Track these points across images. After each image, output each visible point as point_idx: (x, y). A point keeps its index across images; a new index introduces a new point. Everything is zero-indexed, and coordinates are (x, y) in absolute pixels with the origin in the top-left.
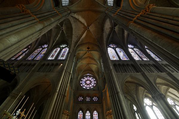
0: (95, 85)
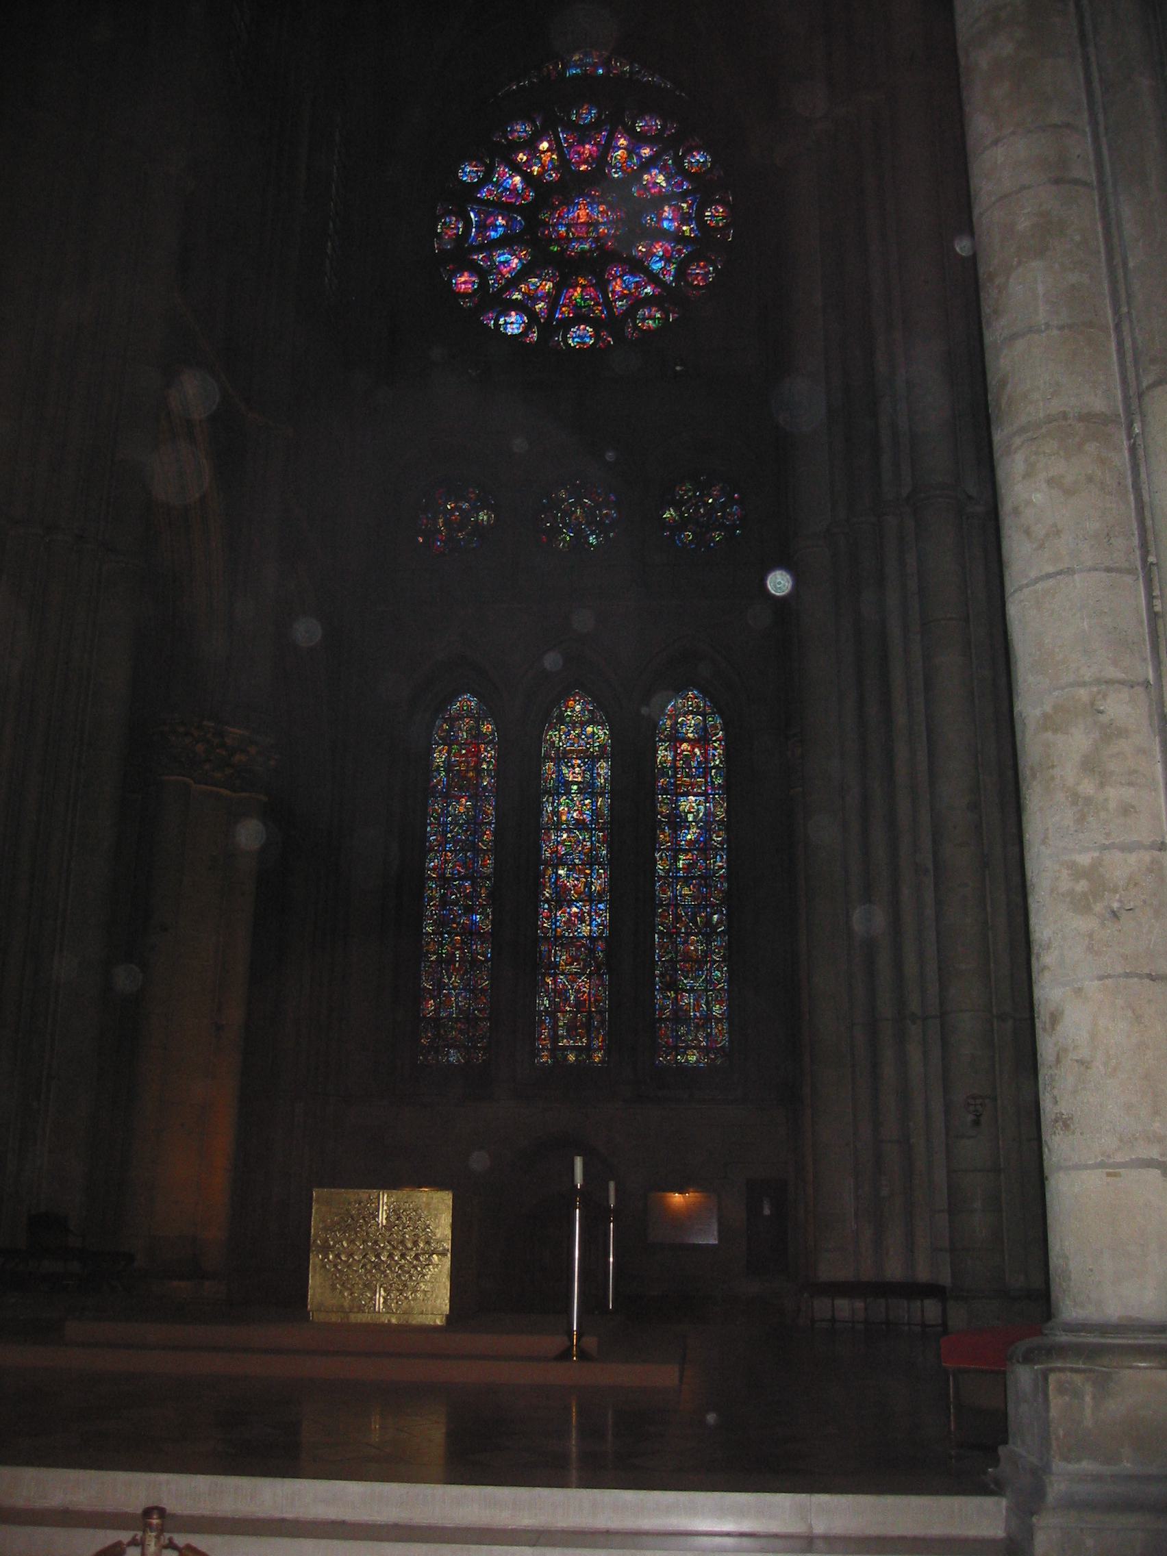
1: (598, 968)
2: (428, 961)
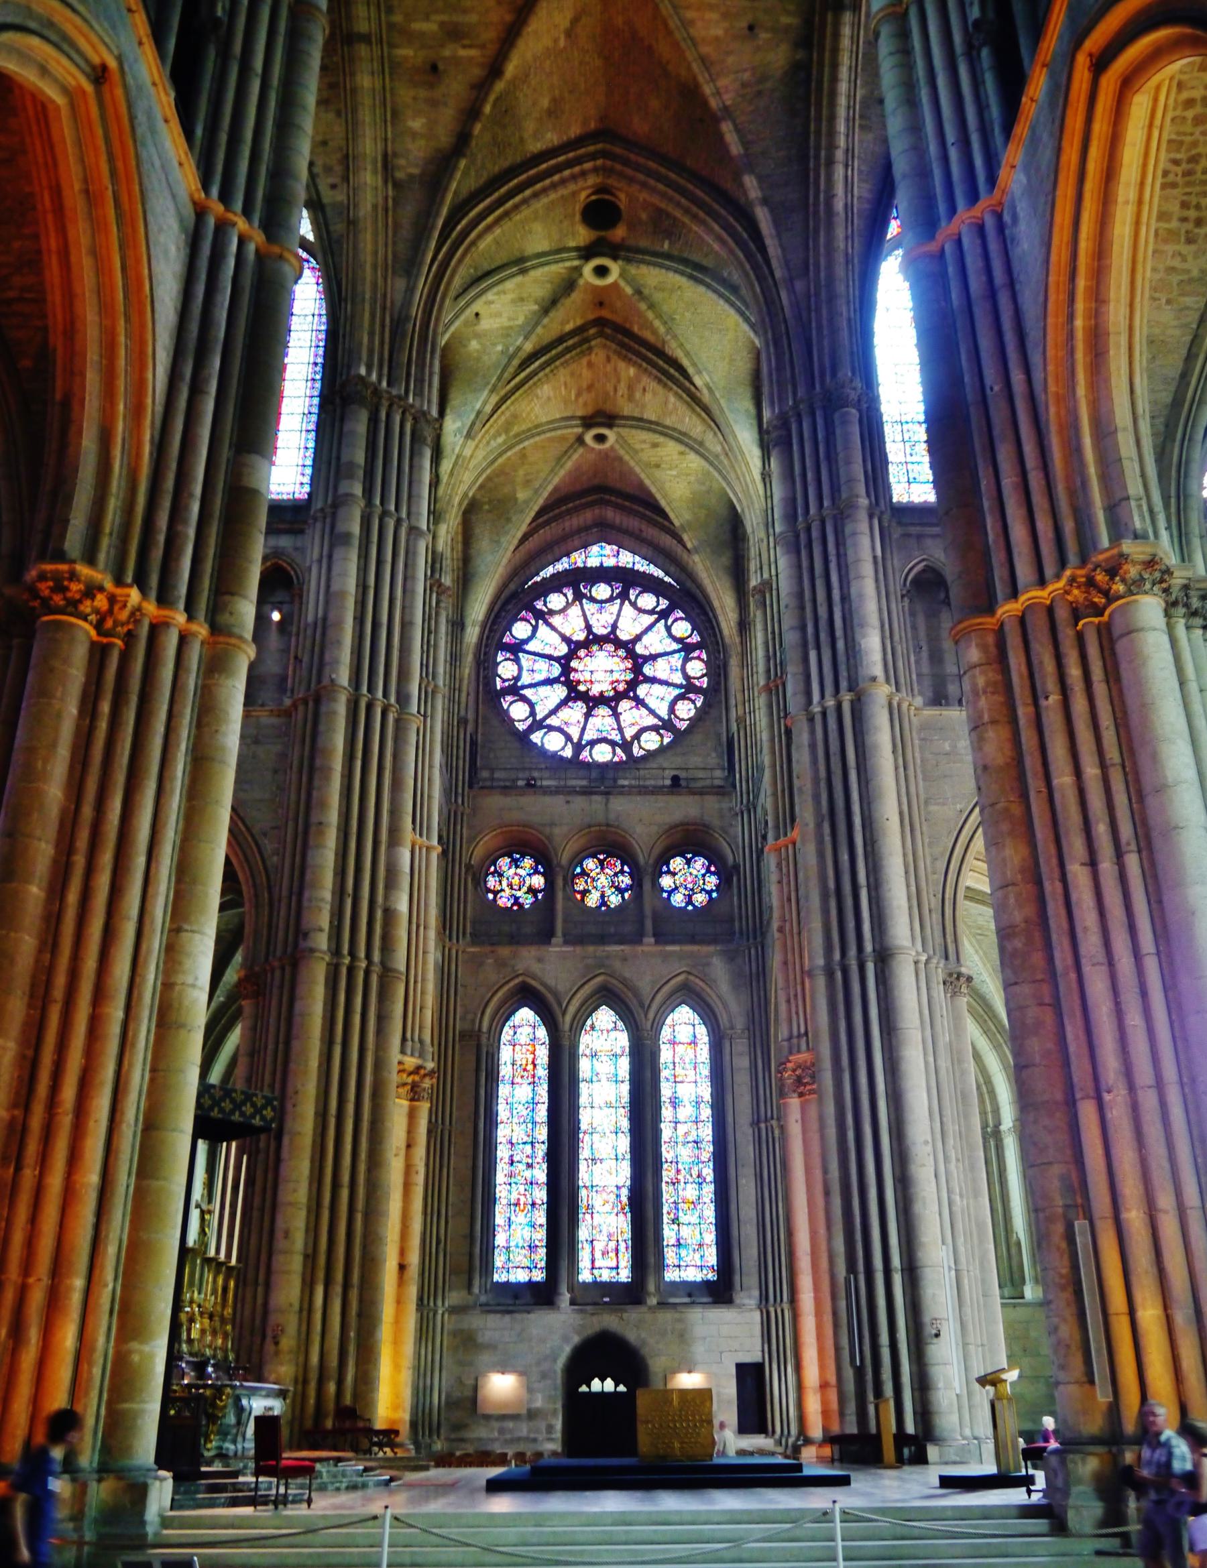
0: (686, 710)
1: (623, 1209)
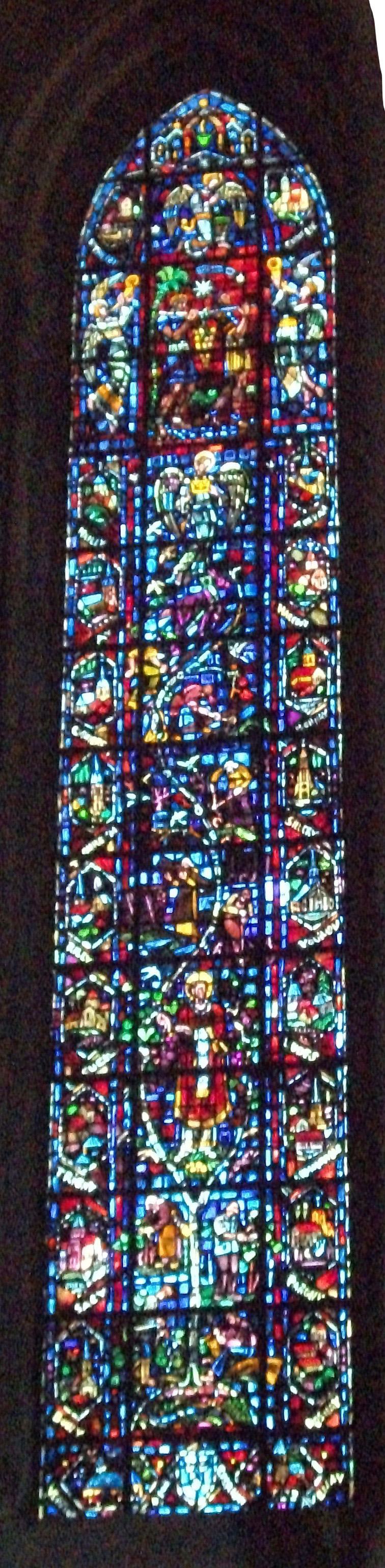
2: (77, 1079)
